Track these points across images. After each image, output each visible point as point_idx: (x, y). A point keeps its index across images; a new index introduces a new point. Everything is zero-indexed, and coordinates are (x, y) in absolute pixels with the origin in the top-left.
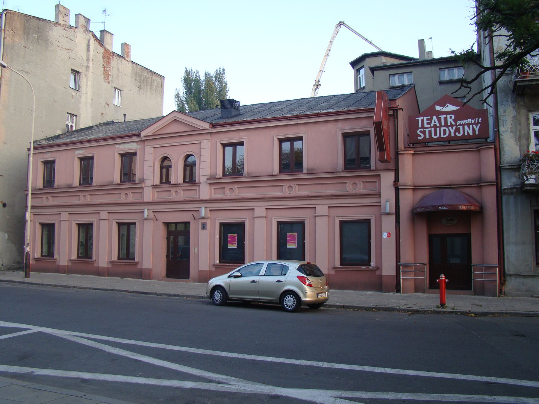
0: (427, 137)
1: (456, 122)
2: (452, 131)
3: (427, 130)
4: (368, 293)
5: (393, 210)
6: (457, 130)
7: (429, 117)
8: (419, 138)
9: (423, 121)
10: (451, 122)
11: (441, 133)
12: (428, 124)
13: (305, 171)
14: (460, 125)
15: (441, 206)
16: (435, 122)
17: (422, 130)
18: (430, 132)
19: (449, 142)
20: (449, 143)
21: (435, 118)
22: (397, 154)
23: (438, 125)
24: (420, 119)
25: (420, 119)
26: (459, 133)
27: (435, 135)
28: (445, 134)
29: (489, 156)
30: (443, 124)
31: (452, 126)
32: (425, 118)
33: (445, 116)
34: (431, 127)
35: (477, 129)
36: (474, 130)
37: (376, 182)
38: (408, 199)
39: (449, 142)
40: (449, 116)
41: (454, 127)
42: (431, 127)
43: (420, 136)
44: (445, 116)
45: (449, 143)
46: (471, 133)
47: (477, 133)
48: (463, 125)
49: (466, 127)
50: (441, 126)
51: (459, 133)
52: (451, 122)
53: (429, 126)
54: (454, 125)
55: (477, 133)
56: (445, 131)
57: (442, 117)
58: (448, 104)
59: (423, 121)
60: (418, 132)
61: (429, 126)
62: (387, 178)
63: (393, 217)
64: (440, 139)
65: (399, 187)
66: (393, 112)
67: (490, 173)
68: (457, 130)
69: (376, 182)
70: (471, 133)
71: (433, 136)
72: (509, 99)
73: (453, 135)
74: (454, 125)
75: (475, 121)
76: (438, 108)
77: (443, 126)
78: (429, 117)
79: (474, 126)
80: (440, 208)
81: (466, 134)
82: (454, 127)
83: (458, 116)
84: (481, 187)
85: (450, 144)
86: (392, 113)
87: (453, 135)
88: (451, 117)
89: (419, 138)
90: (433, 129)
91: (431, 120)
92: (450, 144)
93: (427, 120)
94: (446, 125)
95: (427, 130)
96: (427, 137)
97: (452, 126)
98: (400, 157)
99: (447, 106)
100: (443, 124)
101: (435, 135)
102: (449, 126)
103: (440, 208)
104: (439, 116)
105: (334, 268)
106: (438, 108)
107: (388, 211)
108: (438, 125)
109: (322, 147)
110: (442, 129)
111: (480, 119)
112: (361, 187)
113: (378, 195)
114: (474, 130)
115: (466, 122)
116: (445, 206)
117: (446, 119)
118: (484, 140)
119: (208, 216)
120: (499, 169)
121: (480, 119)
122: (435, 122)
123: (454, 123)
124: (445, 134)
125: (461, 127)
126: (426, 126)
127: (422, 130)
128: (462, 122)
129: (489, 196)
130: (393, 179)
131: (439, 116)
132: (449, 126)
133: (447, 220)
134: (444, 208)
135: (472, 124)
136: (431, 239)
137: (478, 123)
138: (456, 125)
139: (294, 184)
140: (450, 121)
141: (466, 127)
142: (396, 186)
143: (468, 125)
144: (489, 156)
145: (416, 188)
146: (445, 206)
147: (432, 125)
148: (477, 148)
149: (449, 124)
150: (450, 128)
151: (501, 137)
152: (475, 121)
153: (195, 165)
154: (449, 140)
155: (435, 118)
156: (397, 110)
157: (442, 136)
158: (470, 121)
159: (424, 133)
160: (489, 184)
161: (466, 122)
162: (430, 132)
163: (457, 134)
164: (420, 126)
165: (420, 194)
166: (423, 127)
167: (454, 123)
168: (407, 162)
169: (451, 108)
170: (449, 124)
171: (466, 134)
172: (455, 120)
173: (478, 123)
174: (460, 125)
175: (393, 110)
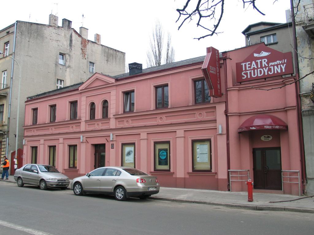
0: (249, 77)
1: (268, 65)
2: (266, 71)
3: (248, 72)
4: (163, 194)
5: (225, 132)
6: (270, 70)
7: (250, 63)
8: (243, 78)
9: (245, 65)
10: (265, 65)
11: (258, 74)
12: (249, 67)
13: (169, 107)
14: (271, 66)
15: (252, 127)
16: (254, 65)
17: (245, 72)
18: (250, 73)
19: (265, 79)
20: (265, 80)
21: (253, 63)
22: (227, 91)
23: (256, 67)
24: (243, 64)
25: (243, 64)
26: (271, 72)
27: (254, 75)
28: (261, 73)
29: (291, 89)
30: (259, 66)
31: (265, 67)
32: (247, 63)
33: (261, 60)
34: (251, 70)
35: (283, 68)
36: (281, 69)
37: (195, 114)
38: (235, 124)
39: (265, 79)
40: (263, 60)
41: (267, 68)
42: (251, 70)
43: (244, 77)
44: (261, 60)
45: (265, 80)
46: (279, 71)
47: (284, 71)
48: (274, 66)
49: (275, 67)
50: (258, 68)
51: (271, 72)
52: (265, 65)
53: (250, 69)
54: (267, 67)
55: (284, 71)
56: (261, 71)
57: (259, 61)
58: (262, 52)
59: (245, 65)
60: (243, 74)
61: (250, 69)
62: (221, 109)
63: (225, 136)
64: (258, 79)
65: (228, 115)
66: (224, 61)
67: (292, 101)
68: (270, 70)
69: (214, 111)
70: (279, 71)
71: (253, 76)
72: (306, 42)
73: (266, 74)
74: (267, 67)
75: (282, 62)
76: (256, 55)
77: (259, 68)
78: (250, 63)
79: (282, 65)
80: (251, 128)
81: (276, 72)
82: (267, 68)
83: (270, 59)
84: (286, 111)
85: (265, 81)
86: (223, 62)
87: (266, 74)
88: (265, 61)
89: (243, 78)
90: (252, 71)
91: (251, 64)
92: (265, 81)
93: (249, 64)
94: (262, 67)
95: (248, 72)
96: (249, 77)
97: (265, 67)
98: (228, 93)
99: (262, 53)
100: (259, 66)
101: (254, 75)
102: (264, 67)
103: (251, 128)
104: (257, 61)
105: (188, 173)
106: (256, 55)
107: (220, 132)
108: (256, 67)
109: (181, 91)
110: (259, 70)
111: (286, 60)
112: (205, 116)
113: (215, 121)
114: (281, 69)
115: (276, 63)
116: (254, 126)
117: (261, 63)
118: (290, 75)
119: (26, 144)
120: (299, 97)
121: (286, 60)
122: (254, 65)
123: (267, 65)
124: (261, 73)
125: (272, 67)
126: (247, 69)
127: (245, 72)
128: (273, 64)
129: (291, 119)
130: (224, 109)
131: (257, 61)
132: (264, 67)
133: (265, 137)
134: (254, 128)
135: (280, 64)
136: (254, 151)
137: (284, 63)
138: (268, 66)
139: (164, 116)
140: (264, 63)
141: (276, 67)
142: (226, 114)
143: (277, 65)
144: (291, 89)
145: (240, 115)
146: (254, 126)
147: (252, 68)
148: (283, 81)
149: (263, 66)
150: (264, 69)
151: (300, 72)
152: (282, 62)
153: (38, 109)
154: (265, 78)
155: (253, 63)
156: (226, 59)
157: (259, 75)
158: (278, 62)
159: (246, 74)
160: (292, 108)
161: (276, 63)
162: (250, 73)
163: (269, 72)
164: (244, 70)
165: (244, 119)
166: (246, 70)
167: (267, 65)
168: (233, 96)
169: (264, 54)
170: (263, 66)
171: (276, 72)
172: (268, 63)
173: (284, 63)
174: (271, 66)
175: (224, 60)
